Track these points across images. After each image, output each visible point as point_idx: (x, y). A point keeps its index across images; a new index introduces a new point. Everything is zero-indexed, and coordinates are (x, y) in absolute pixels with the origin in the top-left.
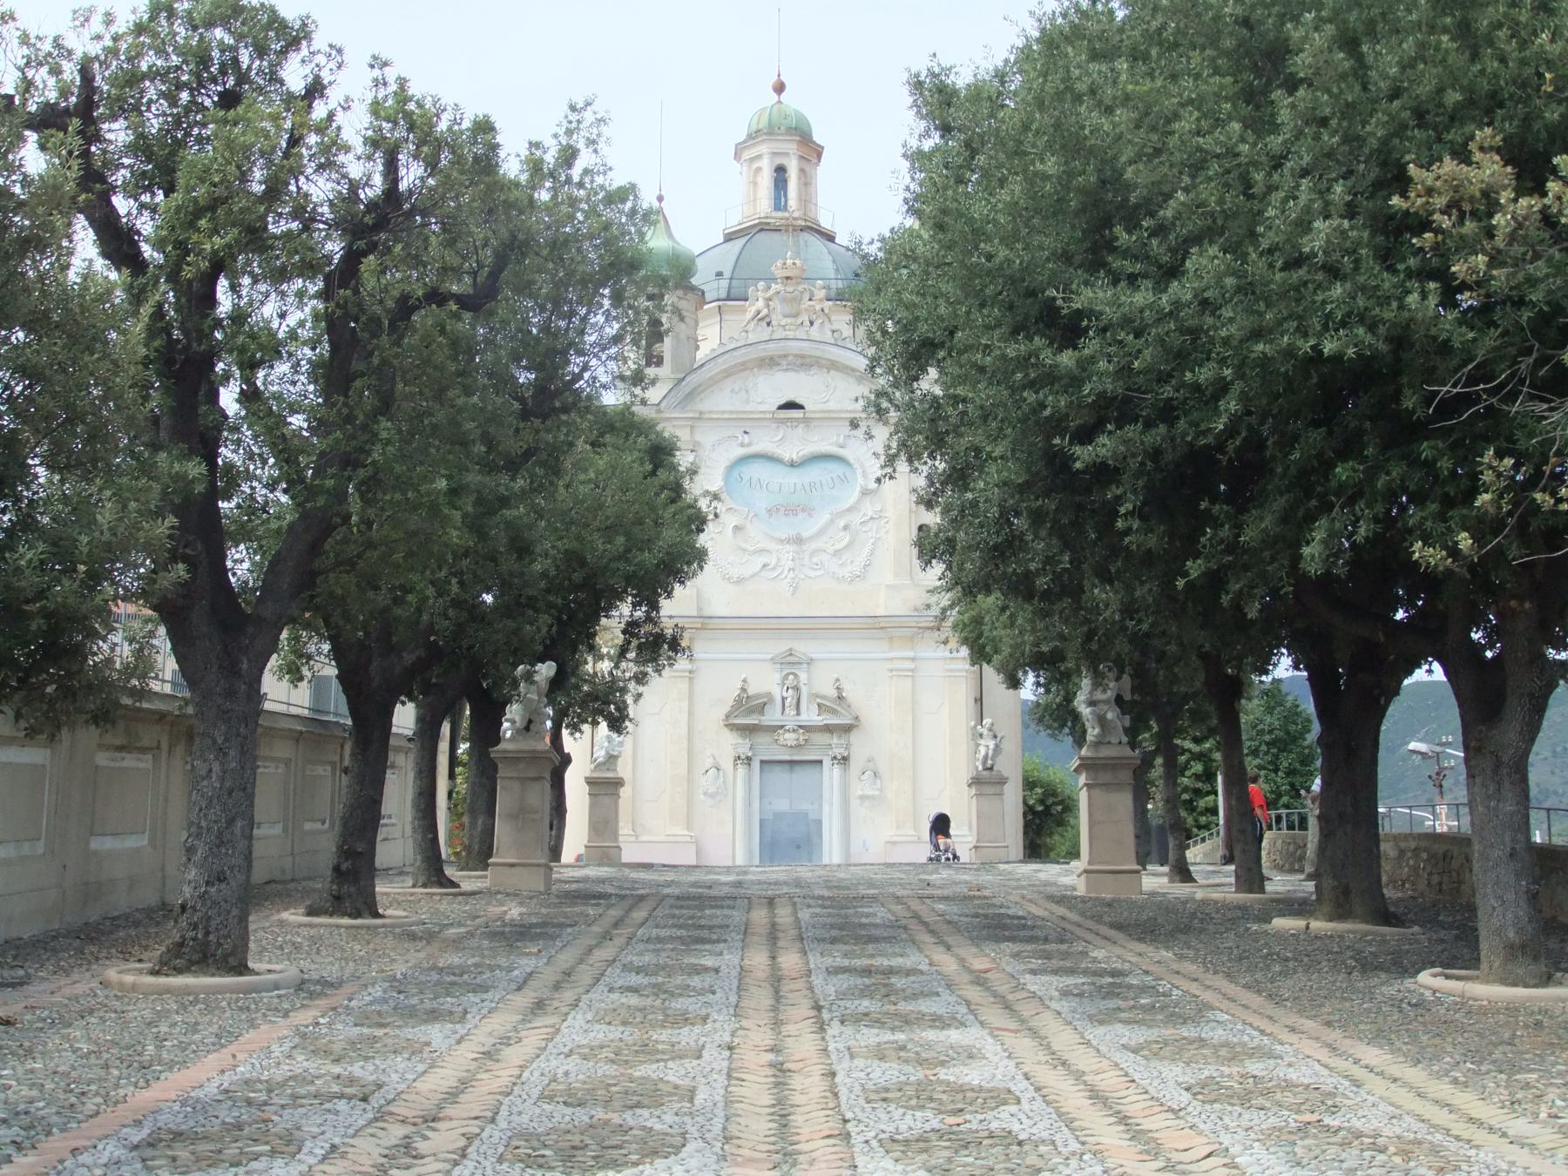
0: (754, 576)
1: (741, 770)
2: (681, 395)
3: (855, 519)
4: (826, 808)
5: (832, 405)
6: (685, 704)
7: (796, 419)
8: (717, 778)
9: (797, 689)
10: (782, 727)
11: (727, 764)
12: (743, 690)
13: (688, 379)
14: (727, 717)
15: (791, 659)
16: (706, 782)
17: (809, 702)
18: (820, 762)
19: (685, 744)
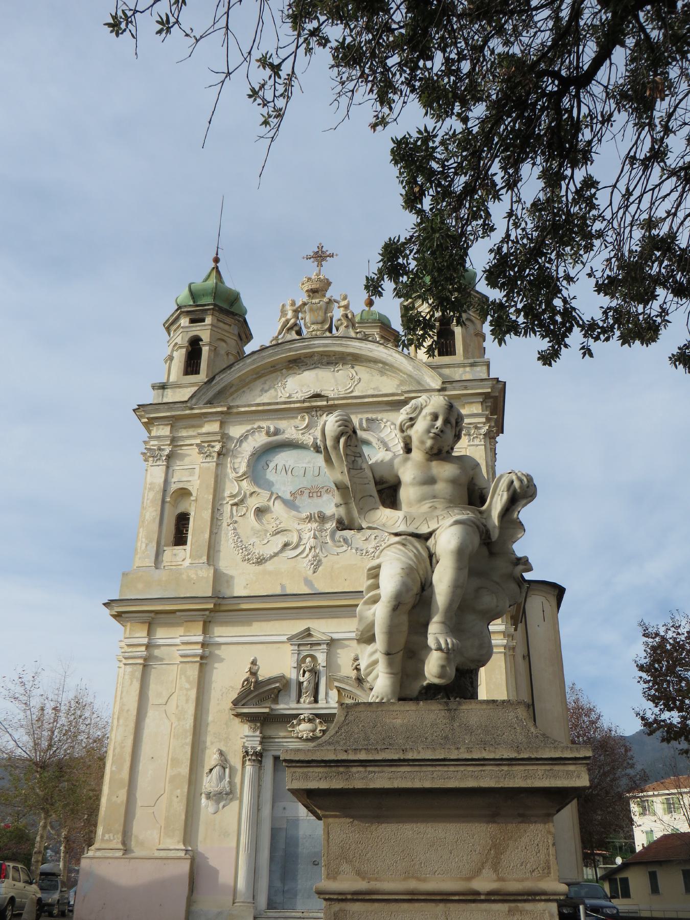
0: (276, 555)
1: (249, 769)
2: (210, 394)
6: (193, 694)
7: (320, 407)
8: (221, 778)
9: (315, 672)
10: (296, 716)
11: (235, 760)
12: (254, 673)
13: (217, 379)
14: (236, 703)
16: (209, 783)
17: (328, 687)
19: (189, 739)
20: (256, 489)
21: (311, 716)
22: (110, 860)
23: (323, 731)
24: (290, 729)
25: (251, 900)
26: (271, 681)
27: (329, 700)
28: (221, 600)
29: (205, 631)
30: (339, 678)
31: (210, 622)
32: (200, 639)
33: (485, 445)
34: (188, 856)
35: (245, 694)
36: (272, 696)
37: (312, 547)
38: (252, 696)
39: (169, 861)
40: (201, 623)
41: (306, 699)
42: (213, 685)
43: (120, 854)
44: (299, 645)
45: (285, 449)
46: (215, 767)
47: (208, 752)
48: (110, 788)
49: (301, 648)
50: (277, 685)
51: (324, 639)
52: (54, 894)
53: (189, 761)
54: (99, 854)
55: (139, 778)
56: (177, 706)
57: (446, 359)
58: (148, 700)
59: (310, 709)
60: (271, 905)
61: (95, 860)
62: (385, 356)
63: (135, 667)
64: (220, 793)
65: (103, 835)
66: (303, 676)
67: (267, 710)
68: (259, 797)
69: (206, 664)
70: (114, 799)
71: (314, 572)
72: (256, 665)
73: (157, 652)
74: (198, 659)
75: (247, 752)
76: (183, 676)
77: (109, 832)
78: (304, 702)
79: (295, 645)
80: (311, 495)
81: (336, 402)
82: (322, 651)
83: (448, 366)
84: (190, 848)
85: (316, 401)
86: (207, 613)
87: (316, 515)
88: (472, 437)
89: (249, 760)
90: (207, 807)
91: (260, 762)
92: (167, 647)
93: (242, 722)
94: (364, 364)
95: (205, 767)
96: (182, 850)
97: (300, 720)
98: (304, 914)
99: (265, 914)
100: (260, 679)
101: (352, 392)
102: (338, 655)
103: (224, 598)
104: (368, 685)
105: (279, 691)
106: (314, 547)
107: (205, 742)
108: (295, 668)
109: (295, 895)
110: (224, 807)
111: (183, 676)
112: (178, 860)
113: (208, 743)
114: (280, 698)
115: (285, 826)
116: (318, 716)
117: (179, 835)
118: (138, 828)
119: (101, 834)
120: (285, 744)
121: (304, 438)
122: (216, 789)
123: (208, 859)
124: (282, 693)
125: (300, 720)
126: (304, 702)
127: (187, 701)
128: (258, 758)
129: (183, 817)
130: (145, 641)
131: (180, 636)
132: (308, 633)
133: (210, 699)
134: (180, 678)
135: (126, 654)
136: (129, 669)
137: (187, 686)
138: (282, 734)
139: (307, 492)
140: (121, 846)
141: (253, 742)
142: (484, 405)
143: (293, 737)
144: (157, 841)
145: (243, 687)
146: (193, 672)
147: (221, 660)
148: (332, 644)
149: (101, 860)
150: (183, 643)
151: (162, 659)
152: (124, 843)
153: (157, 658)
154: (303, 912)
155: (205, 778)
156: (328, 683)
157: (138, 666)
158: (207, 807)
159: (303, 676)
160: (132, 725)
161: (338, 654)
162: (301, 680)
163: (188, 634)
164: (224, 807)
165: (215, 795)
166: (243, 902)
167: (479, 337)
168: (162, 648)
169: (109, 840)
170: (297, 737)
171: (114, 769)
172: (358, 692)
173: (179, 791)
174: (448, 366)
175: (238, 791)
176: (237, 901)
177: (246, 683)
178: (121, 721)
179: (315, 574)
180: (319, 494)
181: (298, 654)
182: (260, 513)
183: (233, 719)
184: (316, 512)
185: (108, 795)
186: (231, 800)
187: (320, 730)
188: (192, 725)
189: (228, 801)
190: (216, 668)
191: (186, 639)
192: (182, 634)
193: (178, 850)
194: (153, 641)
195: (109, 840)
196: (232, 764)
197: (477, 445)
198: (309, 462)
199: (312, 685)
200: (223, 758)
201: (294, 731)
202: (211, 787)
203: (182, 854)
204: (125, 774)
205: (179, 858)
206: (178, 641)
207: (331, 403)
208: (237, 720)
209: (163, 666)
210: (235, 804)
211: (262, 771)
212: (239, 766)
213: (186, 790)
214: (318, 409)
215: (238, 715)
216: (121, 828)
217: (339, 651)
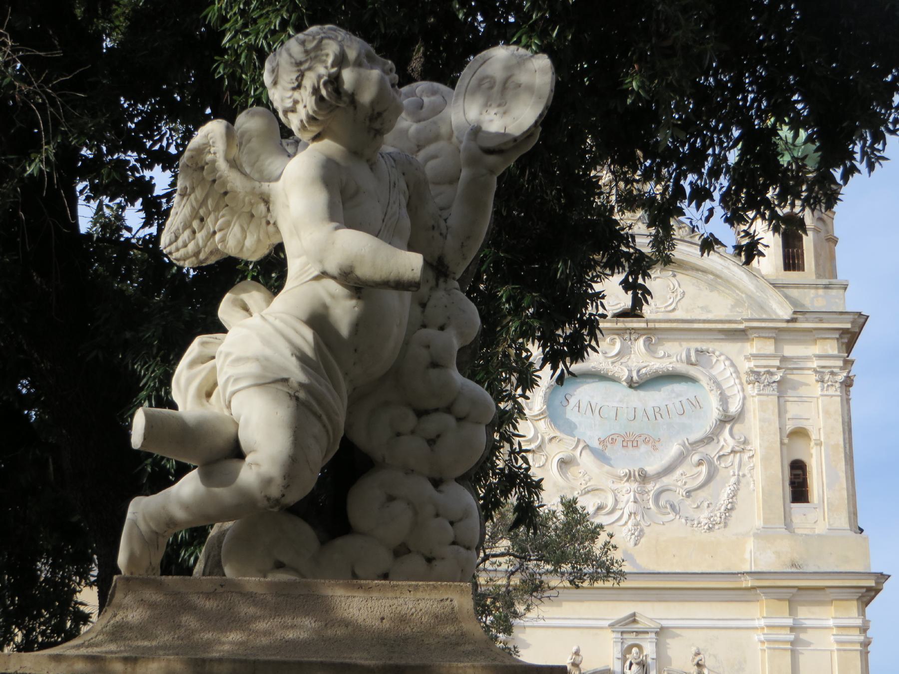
3: (712, 451)
5: (679, 314)
15: (636, 627)
20: (558, 434)
33: (841, 396)
37: (631, 513)
44: (622, 633)
45: (589, 380)
49: (625, 636)
51: (653, 626)
57: (793, 276)
62: (719, 267)
66: (630, 669)
79: (618, 632)
80: (625, 444)
81: (658, 325)
83: (797, 286)
85: (632, 322)
87: (637, 474)
88: (826, 385)
94: (690, 272)
101: (674, 310)
106: (635, 513)
108: (619, 659)
121: (616, 369)
139: (620, 440)
142: (840, 342)
148: (661, 632)
159: (630, 669)
161: (668, 644)
167: (831, 243)
174: (797, 286)
179: (636, 547)
180: (635, 444)
181: (622, 643)
182: (563, 466)
184: (637, 469)
197: (832, 396)
198: (621, 401)
207: (651, 325)
214: (633, 332)
217: (668, 641)
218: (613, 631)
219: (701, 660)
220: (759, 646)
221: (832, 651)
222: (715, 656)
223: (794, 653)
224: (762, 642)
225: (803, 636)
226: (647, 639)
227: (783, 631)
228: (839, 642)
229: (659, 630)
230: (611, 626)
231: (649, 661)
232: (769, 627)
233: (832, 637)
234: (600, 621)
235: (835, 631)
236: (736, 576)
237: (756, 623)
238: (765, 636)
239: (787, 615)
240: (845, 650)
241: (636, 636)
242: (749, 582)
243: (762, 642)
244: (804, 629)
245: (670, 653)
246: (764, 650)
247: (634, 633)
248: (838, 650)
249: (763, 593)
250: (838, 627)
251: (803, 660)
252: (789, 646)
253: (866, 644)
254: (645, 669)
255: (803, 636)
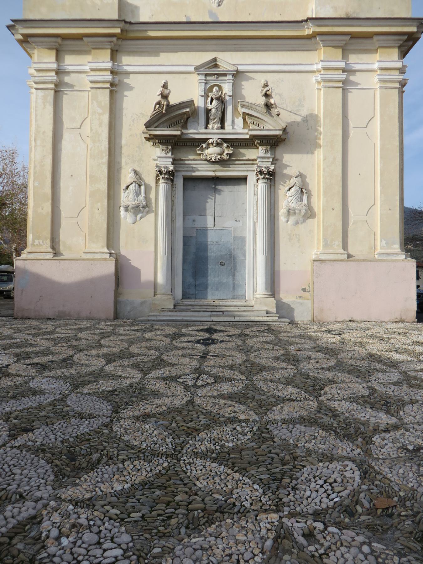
1: (163, 185)
4: (249, 223)
6: (106, 118)
8: (138, 194)
10: (205, 140)
11: (150, 179)
12: (165, 97)
14: (148, 125)
15: (215, 71)
18: (244, 180)
19: (105, 159)
21: (219, 141)
22: (42, 262)
23: (230, 155)
24: (199, 152)
25: (170, 292)
26: (182, 105)
27: (235, 127)
28: (128, 25)
29: (113, 58)
30: (247, 104)
31: (117, 51)
32: (109, 65)
34: (112, 258)
35: (160, 115)
36: (182, 121)
38: (164, 119)
39: (96, 262)
40: (109, 52)
41: (214, 126)
42: (125, 112)
43: (51, 256)
44: (206, 75)
46: (132, 183)
47: (123, 171)
48: (34, 201)
49: (208, 78)
50: (188, 110)
51: (230, 69)
52: (10, 285)
53: (106, 179)
54: (31, 256)
55: (61, 193)
56: (91, 130)
58: (63, 123)
59: (218, 134)
60: (185, 296)
61: (28, 261)
63: (47, 92)
64: (138, 207)
65: (33, 241)
66: (211, 103)
67: (178, 133)
68: (172, 211)
69: (116, 91)
70: (40, 210)
71: (219, 5)
72: (167, 89)
73: (67, 79)
74: (108, 85)
75: (160, 172)
76: (94, 102)
77: (39, 238)
78: (213, 128)
79: (202, 74)
82: (228, 81)
84: (113, 252)
86: (114, 39)
89: (163, 178)
90: (126, 218)
91: (172, 181)
92: (77, 74)
93: (153, 145)
95: (122, 185)
96: (106, 253)
97: (209, 144)
98: (215, 302)
99: (182, 302)
100: (171, 103)
102: (242, 87)
103: (130, 23)
104: (276, 110)
105: (188, 119)
107: (120, 163)
108: (202, 96)
109: (206, 288)
110: (141, 218)
111: (94, 102)
112: (103, 261)
113: (123, 164)
114: (189, 124)
115: (195, 235)
116: (225, 140)
117: (103, 240)
118: (64, 235)
119: (31, 239)
120: (194, 166)
122: (134, 203)
123: (130, 260)
124: (190, 120)
125: (209, 144)
126: (213, 128)
127: (100, 125)
128: (171, 176)
129: (105, 226)
130: (54, 66)
131: (89, 62)
132: (214, 63)
133: (122, 124)
134: (92, 103)
135: (37, 78)
136: (40, 93)
137: (100, 111)
138: (191, 157)
140: (51, 251)
141: (165, 163)
143: (202, 160)
144: (83, 246)
145: (155, 110)
146: (104, 97)
147: (131, 88)
148: (237, 75)
149: (33, 261)
150: (92, 70)
151: (72, 86)
152: (53, 248)
153: (67, 85)
154: (214, 301)
155: (122, 193)
156: (234, 111)
157: (50, 91)
158: (126, 218)
159: (211, 103)
160: (49, 146)
161: (243, 85)
162: (210, 108)
163: (96, 61)
164: (141, 218)
165: (133, 208)
166: (163, 294)
168: (72, 75)
169: (40, 245)
170: (206, 160)
171: (36, 184)
172: (266, 118)
173: (99, 204)
175: (153, 205)
176: (158, 293)
177: (158, 106)
178: (39, 142)
179: (220, 7)
181: (206, 84)
183: (145, 142)
185: (33, 207)
186: (148, 213)
187: (227, 154)
188: (107, 146)
189: (145, 213)
190: (126, 96)
191: (94, 65)
192: (91, 61)
193: (103, 253)
194: (62, 68)
195: (40, 245)
196: (147, 182)
199: (220, 113)
200: (138, 176)
201: (203, 154)
202: (128, 201)
203: (107, 256)
204: (48, 190)
205: (105, 260)
206: (87, 68)
208: (149, 144)
209: (75, 92)
210: (151, 216)
211: (174, 189)
212: (152, 183)
213: (105, 203)
215: (148, 139)
216: (49, 236)
217: (243, 83)
218: (198, 74)
219: (269, 91)
220: (317, 86)
221: (375, 90)
222: (280, 95)
223: (345, 92)
224: (319, 83)
225: (352, 78)
226: (226, 80)
227: (337, 72)
228: (381, 81)
229: (235, 72)
230: (197, 68)
231: (227, 98)
232: (325, 69)
233: (377, 77)
234: (186, 67)
235: (379, 72)
236: (300, 24)
237: (315, 67)
238: (322, 76)
239: (340, 59)
240: (386, 88)
241: (217, 78)
242: (310, 30)
243: (319, 83)
244: (353, 72)
245: (244, 92)
246: (320, 89)
247: (216, 76)
248: (381, 88)
249: (321, 41)
250: (382, 69)
251: (351, 97)
252: (340, 85)
253: (403, 84)
254: (223, 106)
255: (352, 78)
